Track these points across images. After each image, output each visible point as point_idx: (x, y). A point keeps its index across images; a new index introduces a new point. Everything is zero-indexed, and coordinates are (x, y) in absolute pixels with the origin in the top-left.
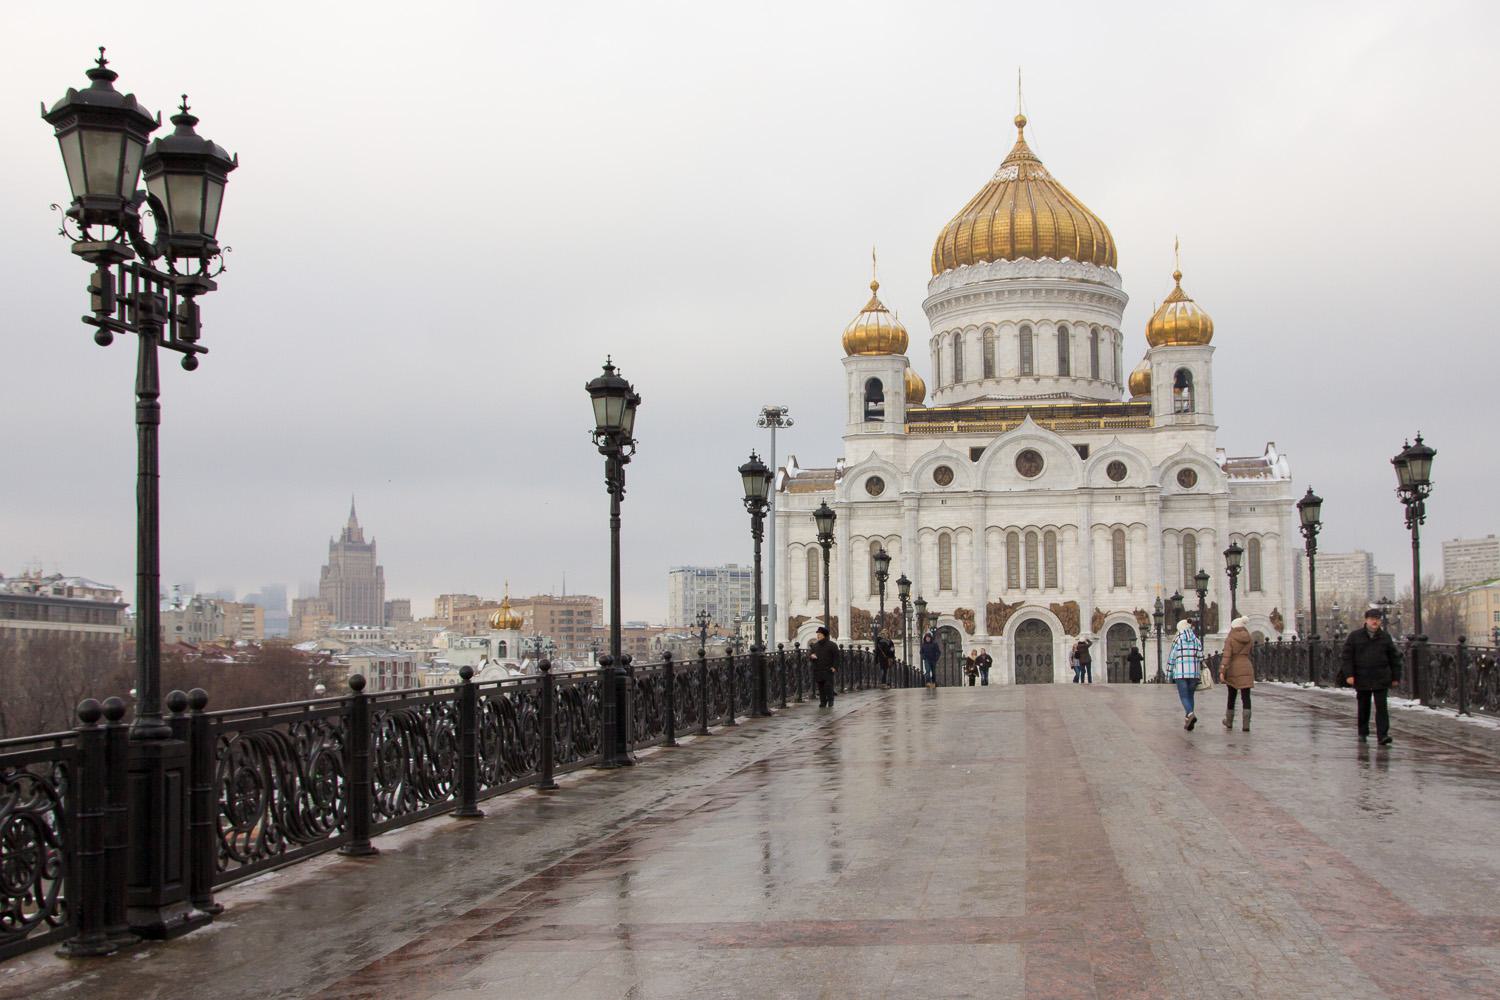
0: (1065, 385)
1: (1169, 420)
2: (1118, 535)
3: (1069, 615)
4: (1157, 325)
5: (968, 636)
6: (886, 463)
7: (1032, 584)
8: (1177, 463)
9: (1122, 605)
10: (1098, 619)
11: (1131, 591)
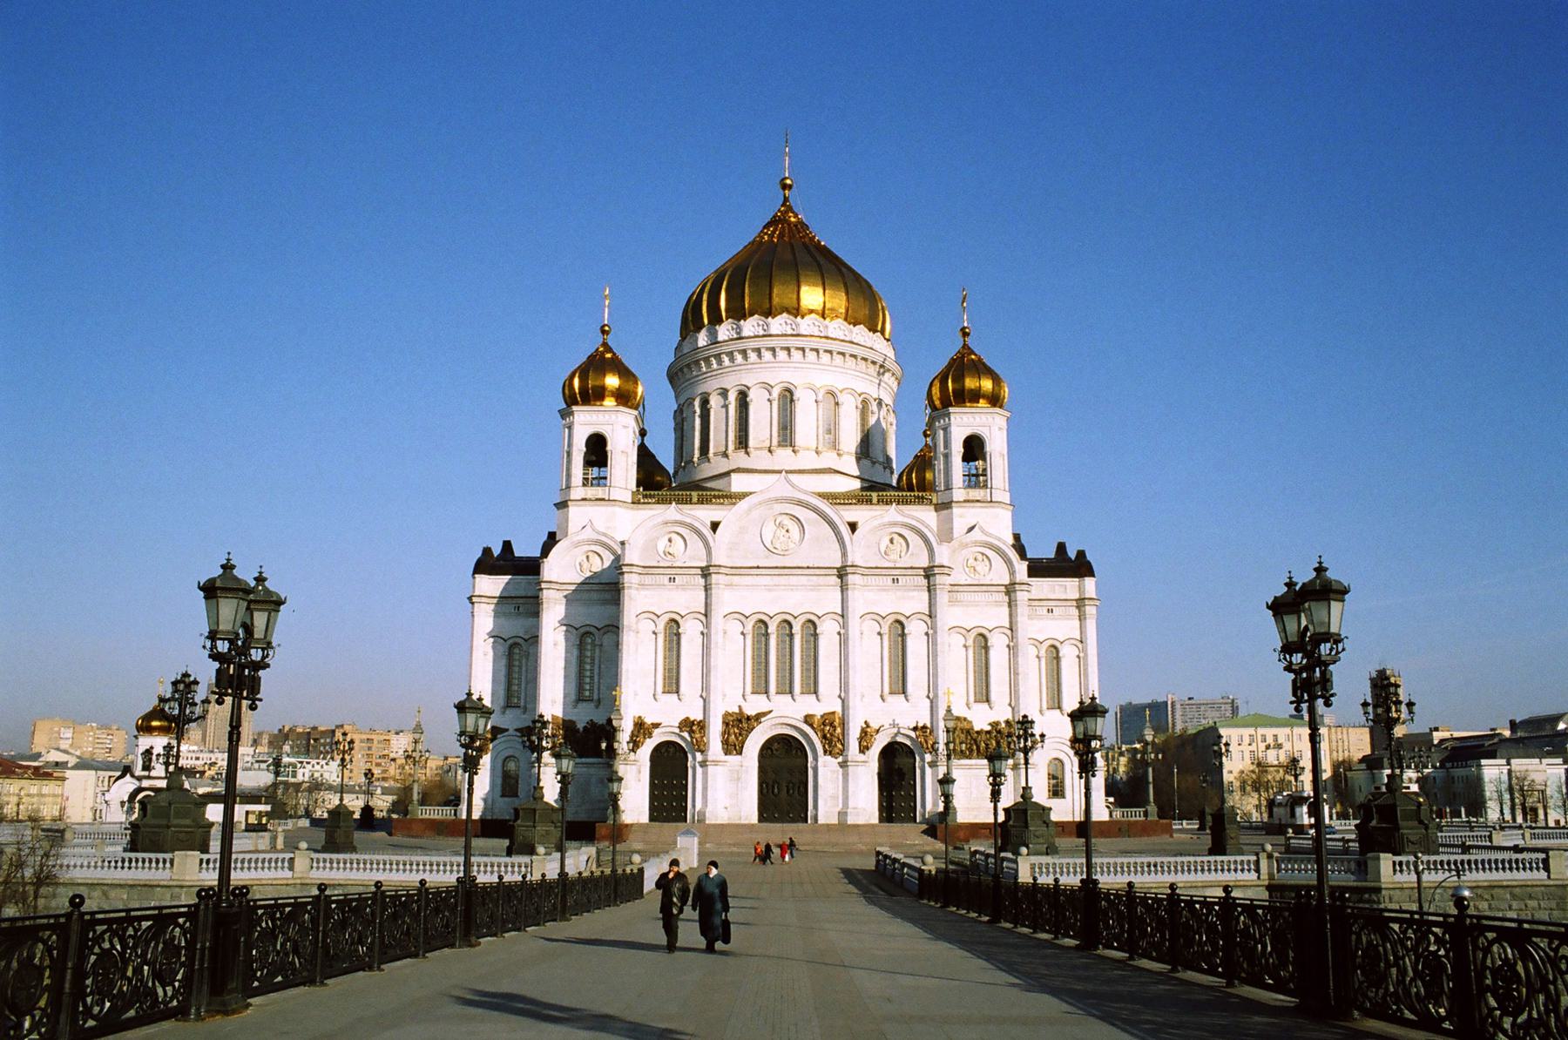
3: (831, 731)
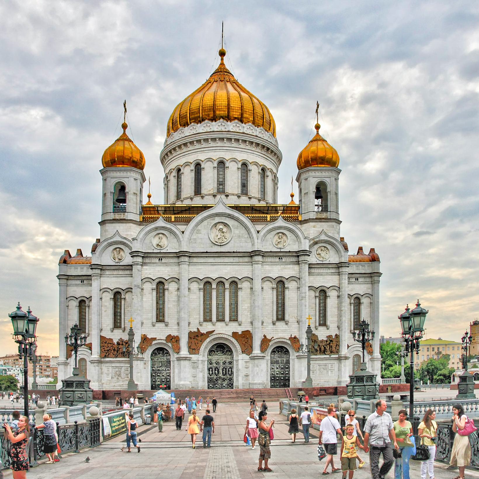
5: (175, 354)
6: (125, 238)
10: (265, 342)
11: (287, 324)
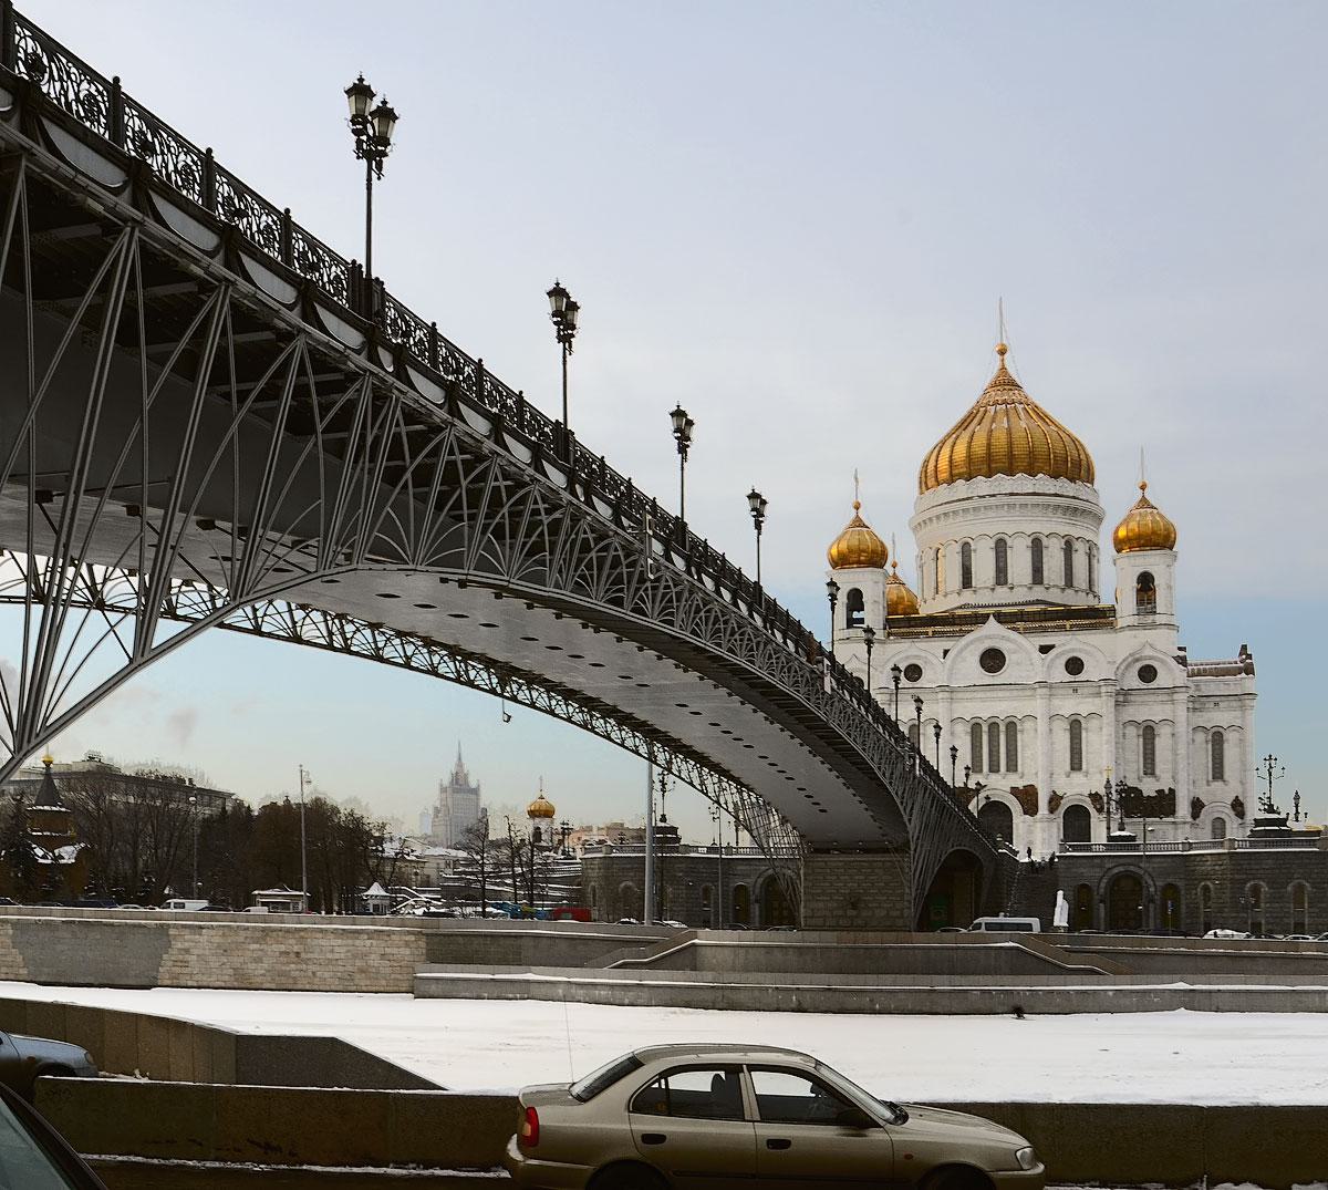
0: (1038, 593)
1: (1134, 620)
2: (1075, 727)
3: (1028, 798)
4: (1122, 533)
7: (994, 768)
8: (1137, 660)
9: (1077, 788)
10: (1055, 801)
